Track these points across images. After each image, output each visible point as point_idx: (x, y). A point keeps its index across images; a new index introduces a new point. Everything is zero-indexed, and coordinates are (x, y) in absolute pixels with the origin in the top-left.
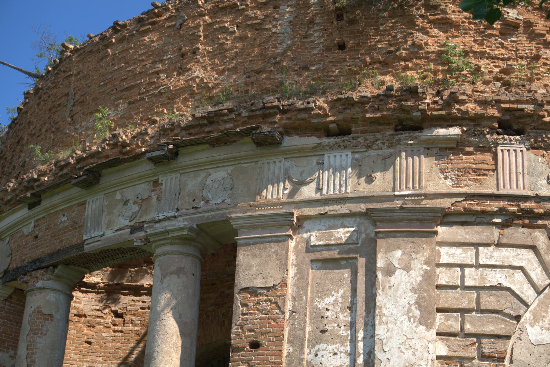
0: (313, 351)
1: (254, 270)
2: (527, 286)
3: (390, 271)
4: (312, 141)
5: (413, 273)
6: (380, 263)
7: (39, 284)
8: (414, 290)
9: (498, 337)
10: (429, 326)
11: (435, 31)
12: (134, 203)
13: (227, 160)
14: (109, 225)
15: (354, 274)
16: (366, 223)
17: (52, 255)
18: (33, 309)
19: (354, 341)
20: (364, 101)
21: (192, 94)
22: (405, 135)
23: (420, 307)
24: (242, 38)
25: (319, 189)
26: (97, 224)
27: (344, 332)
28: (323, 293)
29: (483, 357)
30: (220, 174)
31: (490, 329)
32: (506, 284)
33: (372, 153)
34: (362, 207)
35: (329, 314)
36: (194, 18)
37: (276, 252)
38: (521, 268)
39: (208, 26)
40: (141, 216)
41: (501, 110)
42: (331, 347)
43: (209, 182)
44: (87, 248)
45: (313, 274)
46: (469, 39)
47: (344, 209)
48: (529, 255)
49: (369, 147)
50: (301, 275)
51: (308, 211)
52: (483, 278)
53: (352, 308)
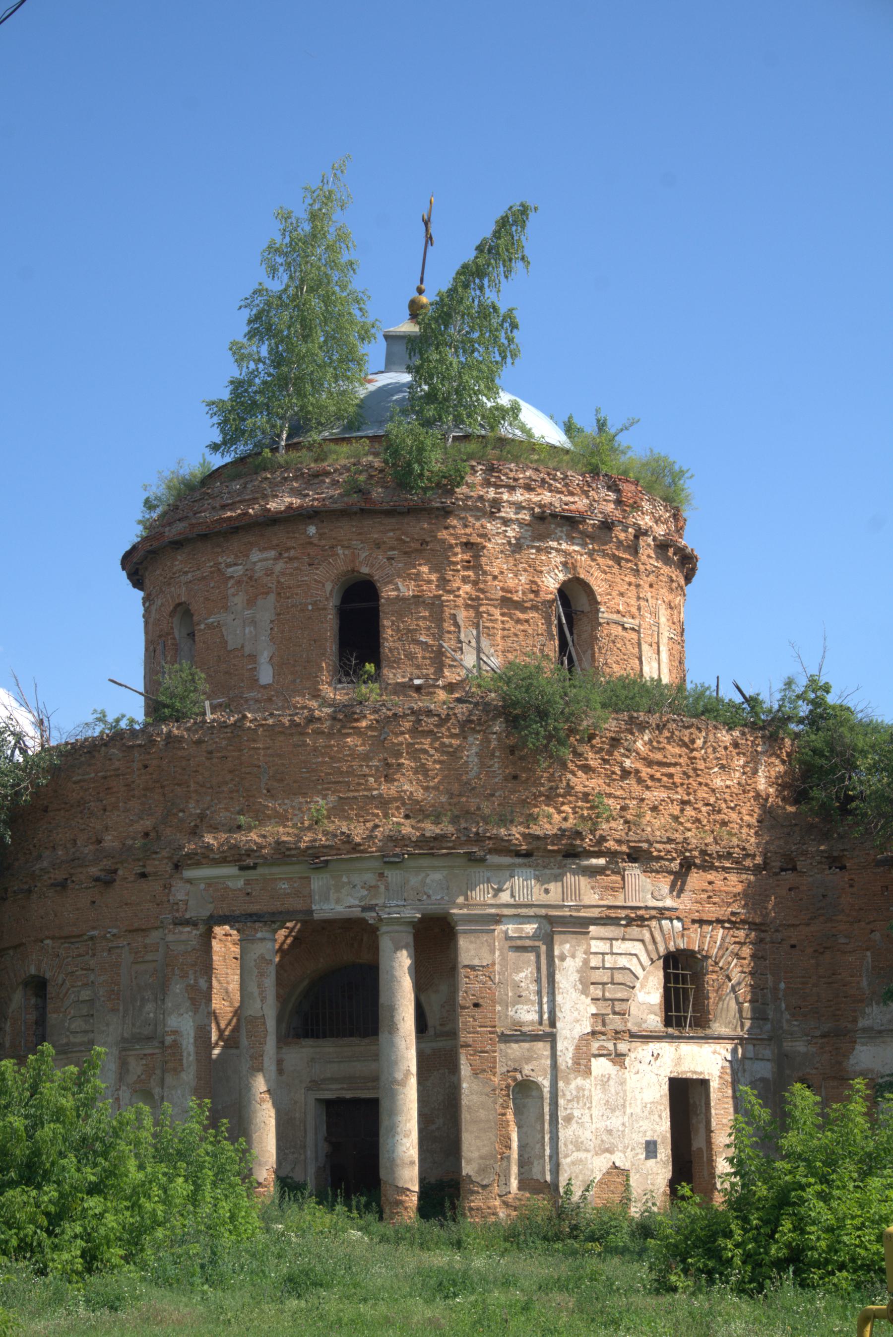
0: (514, 1009)
1: (472, 953)
2: (639, 967)
3: (563, 958)
4: (507, 860)
5: (577, 960)
6: (557, 953)
7: (259, 935)
8: (578, 971)
9: (623, 1000)
10: (587, 996)
11: (580, 773)
12: (362, 888)
13: (444, 867)
14: (338, 901)
15: (538, 957)
16: (545, 922)
17: (273, 914)
18: (257, 955)
19: (540, 1004)
20: (546, 837)
21: (404, 804)
22: (569, 861)
23: (581, 983)
24: (440, 762)
25: (513, 896)
26: (327, 899)
27: (534, 998)
28: (518, 970)
29: (615, 1013)
30: (437, 876)
31: (619, 995)
32: (628, 966)
34: (543, 912)
35: (522, 984)
36: (397, 735)
37: (486, 941)
38: (635, 955)
39: (410, 745)
40: (371, 900)
41: (630, 847)
42: (525, 1007)
43: (428, 881)
44: (316, 916)
45: (512, 955)
46: (601, 781)
47: (531, 912)
48: (639, 945)
49: (545, 867)
50: (503, 958)
51: (506, 911)
52: (615, 962)
53: (538, 981)
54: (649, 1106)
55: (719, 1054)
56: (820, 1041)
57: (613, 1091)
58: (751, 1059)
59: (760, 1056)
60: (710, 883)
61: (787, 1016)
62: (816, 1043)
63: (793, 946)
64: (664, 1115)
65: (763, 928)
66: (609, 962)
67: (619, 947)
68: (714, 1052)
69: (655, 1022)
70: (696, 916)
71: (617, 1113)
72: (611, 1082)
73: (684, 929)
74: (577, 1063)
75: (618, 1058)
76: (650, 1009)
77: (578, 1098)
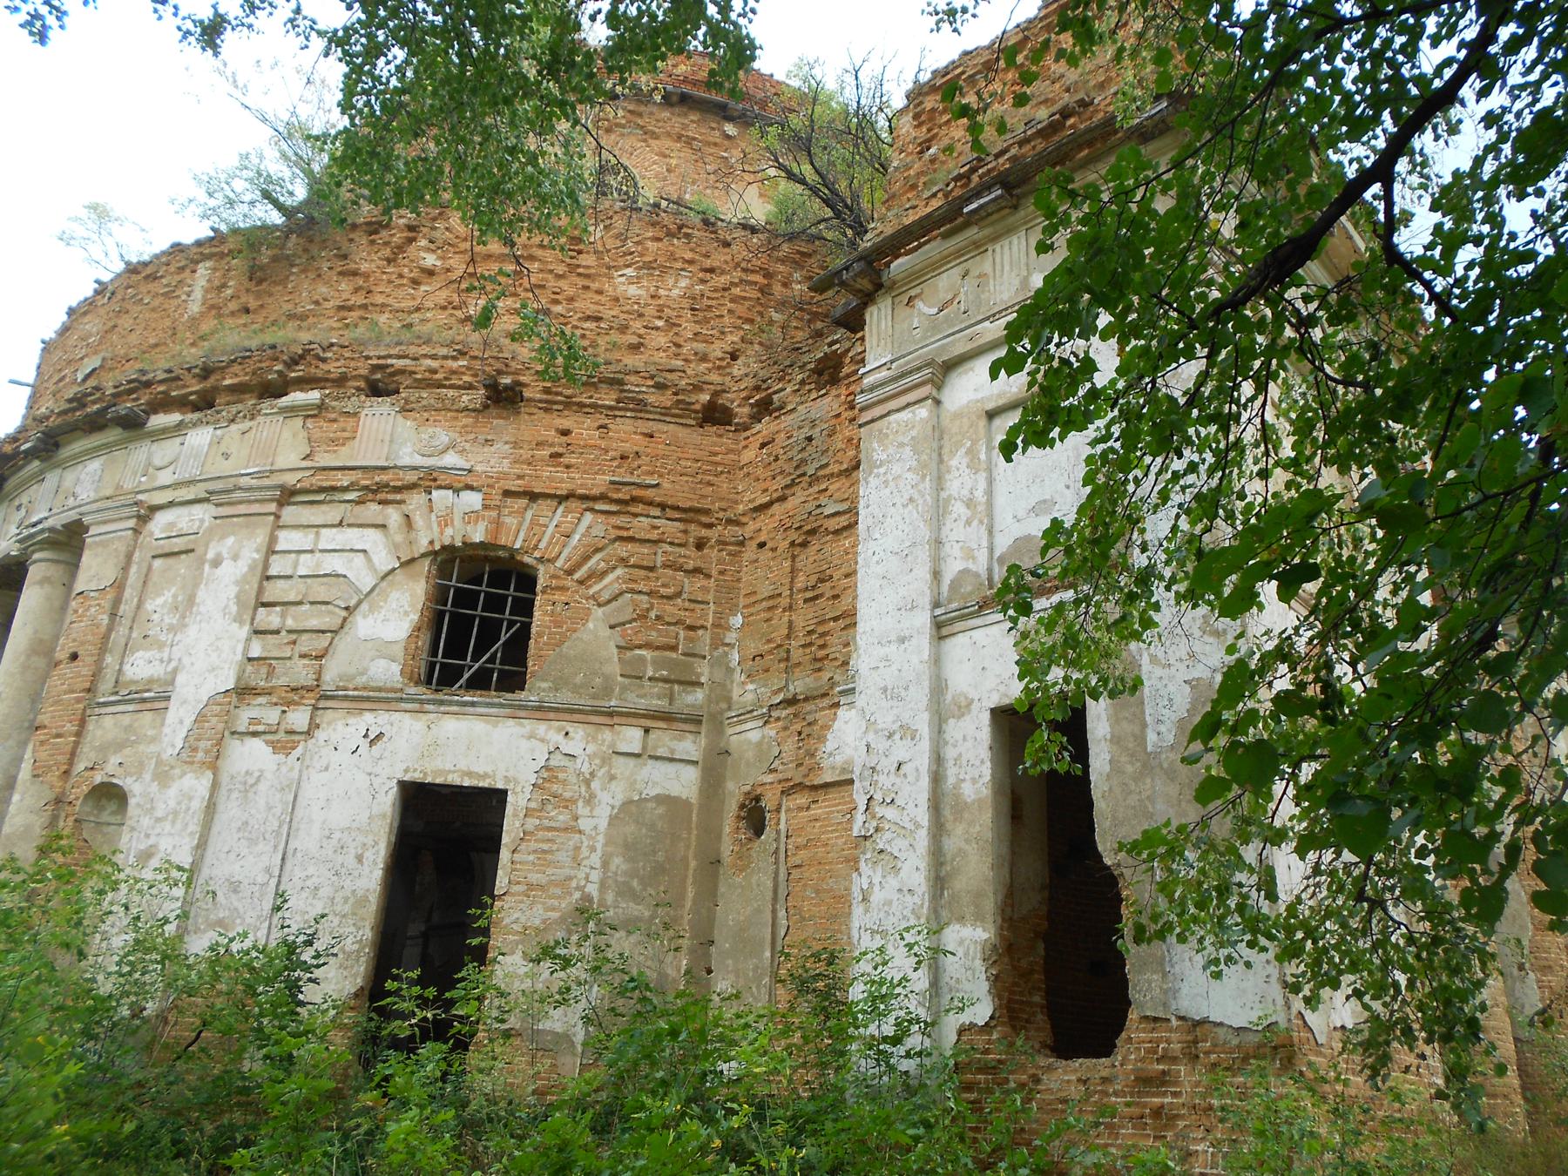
3: (216, 563)
4: (175, 417)
5: (240, 563)
8: (237, 583)
33: (234, 427)
35: (155, 617)
42: (148, 655)
54: (337, 835)
55: (542, 740)
56: (784, 713)
57: (262, 802)
58: (638, 756)
59: (660, 752)
60: (565, 433)
61: (739, 677)
62: (778, 719)
63: (762, 545)
64: (369, 855)
65: (704, 519)
66: (306, 565)
67: (330, 538)
68: (531, 736)
69: (388, 672)
70: (514, 485)
71: (261, 847)
72: (262, 787)
73: (485, 507)
74: (190, 746)
75: (284, 741)
76: (382, 649)
77: (176, 813)
